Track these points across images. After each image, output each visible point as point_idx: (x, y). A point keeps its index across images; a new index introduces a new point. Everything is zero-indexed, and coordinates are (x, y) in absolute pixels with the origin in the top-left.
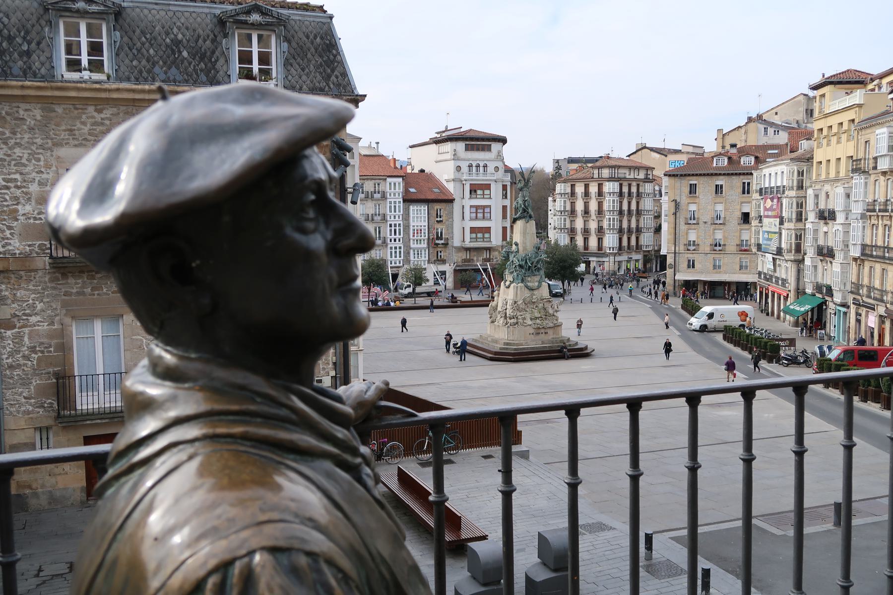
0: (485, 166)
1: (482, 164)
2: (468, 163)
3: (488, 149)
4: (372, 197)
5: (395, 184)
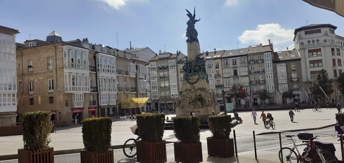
0: (318, 40)
1: (315, 40)
2: (307, 40)
3: (320, 31)
4: (257, 62)
5: (267, 55)
